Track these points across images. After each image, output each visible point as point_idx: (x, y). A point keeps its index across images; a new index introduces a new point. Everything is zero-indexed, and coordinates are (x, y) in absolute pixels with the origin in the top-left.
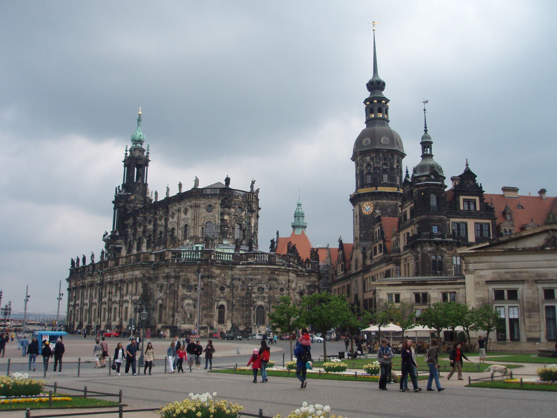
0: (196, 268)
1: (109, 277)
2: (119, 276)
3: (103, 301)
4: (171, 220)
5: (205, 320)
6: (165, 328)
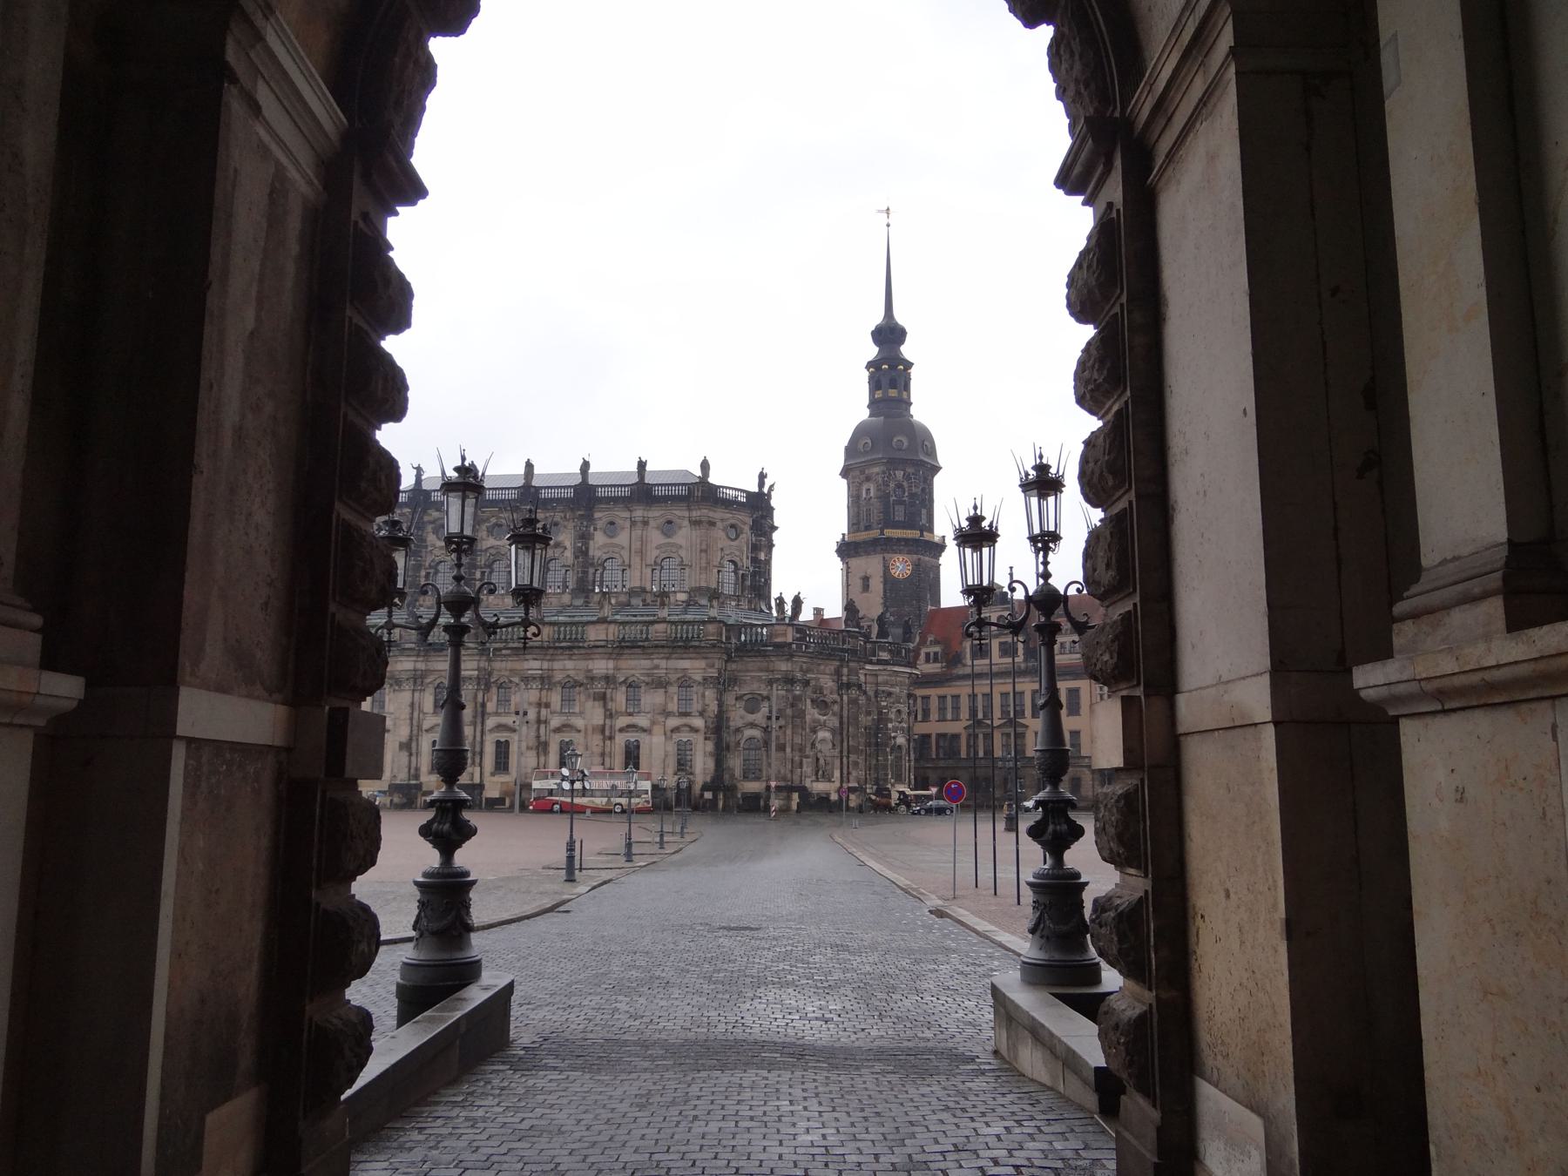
0: (832, 666)
1: (536, 664)
2: (601, 666)
3: (491, 722)
4: (599, 539)
5: (854, 773)
6: (790, 789)
